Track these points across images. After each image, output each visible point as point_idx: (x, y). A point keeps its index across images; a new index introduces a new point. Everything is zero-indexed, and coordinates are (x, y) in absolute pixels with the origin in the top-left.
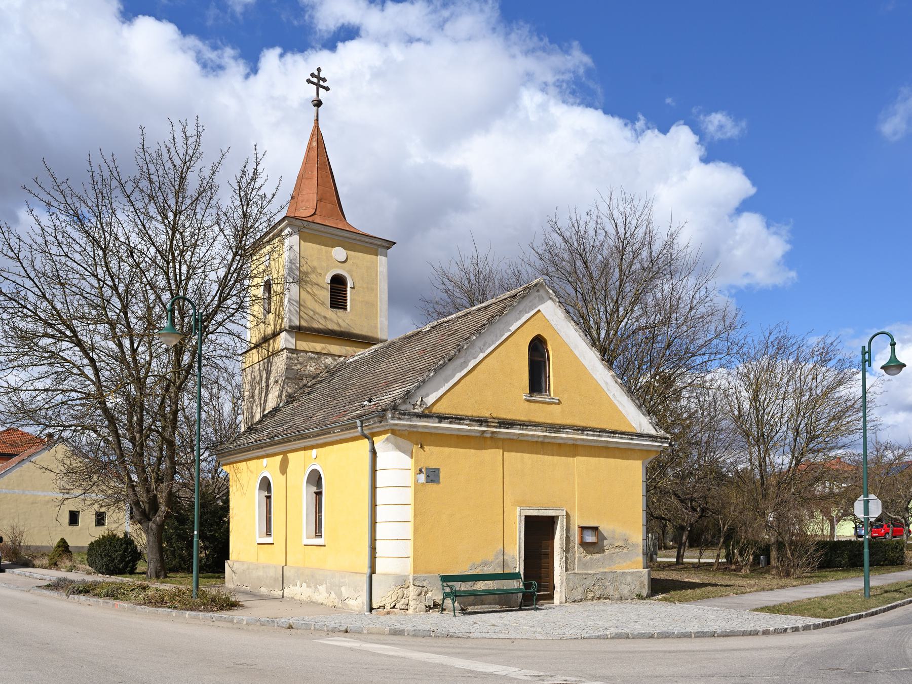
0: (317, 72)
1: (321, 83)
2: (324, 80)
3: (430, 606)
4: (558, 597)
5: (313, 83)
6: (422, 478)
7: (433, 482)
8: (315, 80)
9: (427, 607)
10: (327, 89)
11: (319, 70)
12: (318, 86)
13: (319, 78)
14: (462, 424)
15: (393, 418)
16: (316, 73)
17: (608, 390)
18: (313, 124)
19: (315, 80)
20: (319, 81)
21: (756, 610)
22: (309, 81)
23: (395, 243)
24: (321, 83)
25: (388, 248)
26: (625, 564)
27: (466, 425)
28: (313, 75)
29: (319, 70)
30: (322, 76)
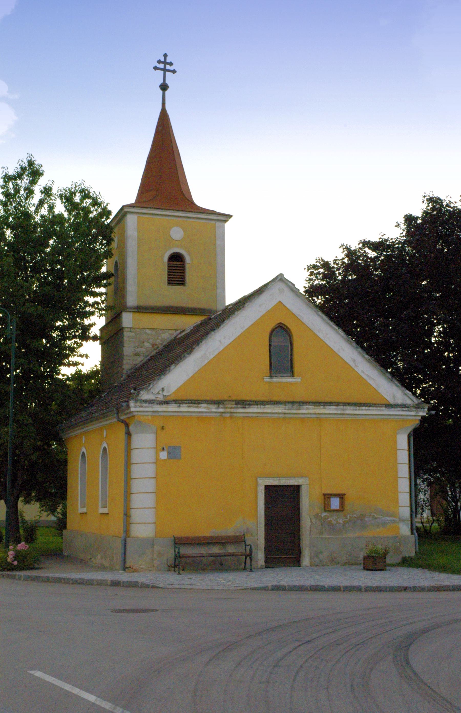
0: (163, 57)
1: (168, 67)
2: (171, 64)
3: (171, 565)
4: (306, 561)
5: (160, 69)
6: (163, 455)
7: (174, 458)
8: (162, 66)
9: (169, 566)
10: (174, 72)
11: (165, 56)
12: (165, 70)
13: (165, 63)
14: (200, 407)
15: (135, 406)
16: (162, 60)
17: (356, 366)
18: (160, 108)
19: (162, 66)
20: (165, 67)
21: (153, 611)
22: (156, 68)
23: (230, 216)
24: (168, 67)
25: (226, 221)
26: (378, 530)
27: (205, 408)
28: (159, 62)
29: (165, 56)
30: (168, 60)
